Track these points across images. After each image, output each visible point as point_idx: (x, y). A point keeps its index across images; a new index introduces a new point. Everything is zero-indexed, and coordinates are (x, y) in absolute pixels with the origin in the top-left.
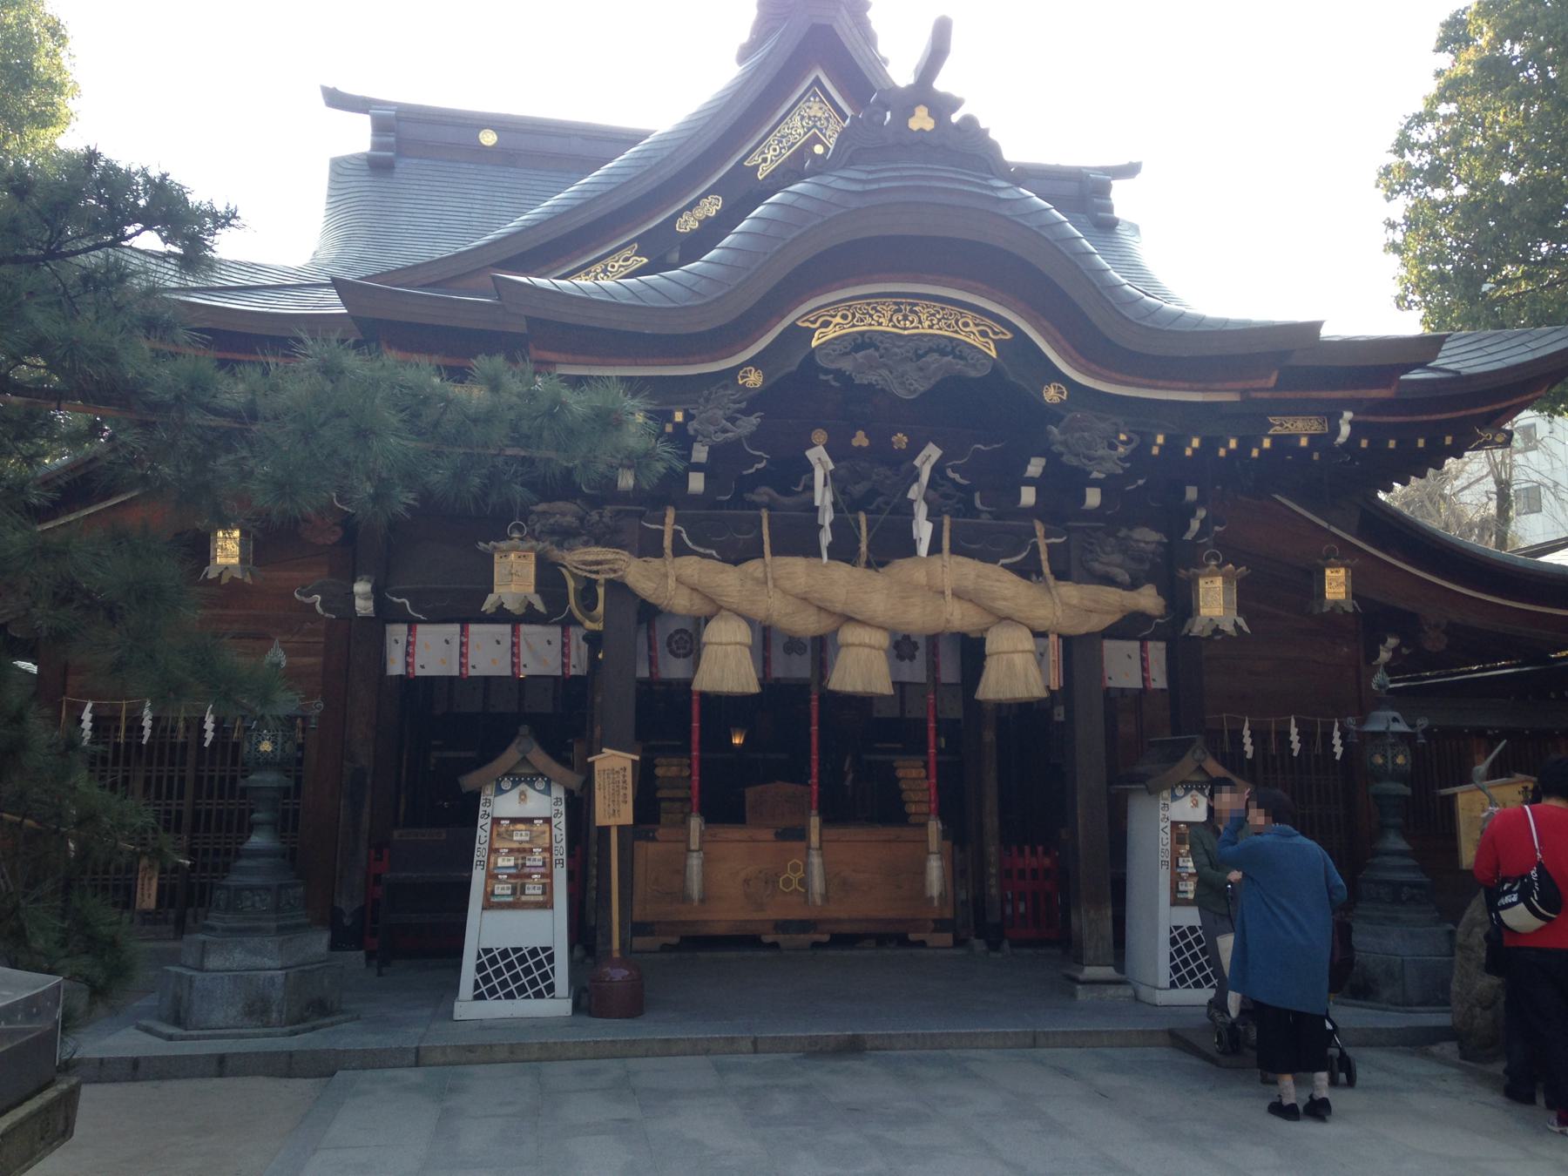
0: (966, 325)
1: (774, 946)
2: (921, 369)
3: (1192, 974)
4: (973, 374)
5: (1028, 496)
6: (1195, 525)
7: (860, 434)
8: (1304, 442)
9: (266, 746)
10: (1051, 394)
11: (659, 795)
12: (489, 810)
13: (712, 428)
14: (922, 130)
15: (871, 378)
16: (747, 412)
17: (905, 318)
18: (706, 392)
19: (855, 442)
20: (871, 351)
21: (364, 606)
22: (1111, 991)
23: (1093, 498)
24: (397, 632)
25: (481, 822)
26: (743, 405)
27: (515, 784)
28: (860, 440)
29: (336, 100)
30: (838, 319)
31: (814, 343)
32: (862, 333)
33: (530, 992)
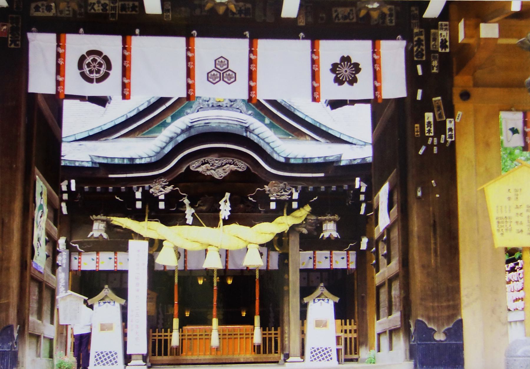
2: (224, 170)
4: (240, 170)
13: (157, 191)
15: (208, 173)
16: (169, 185)
20: (207, 165)
26: (167, 183)
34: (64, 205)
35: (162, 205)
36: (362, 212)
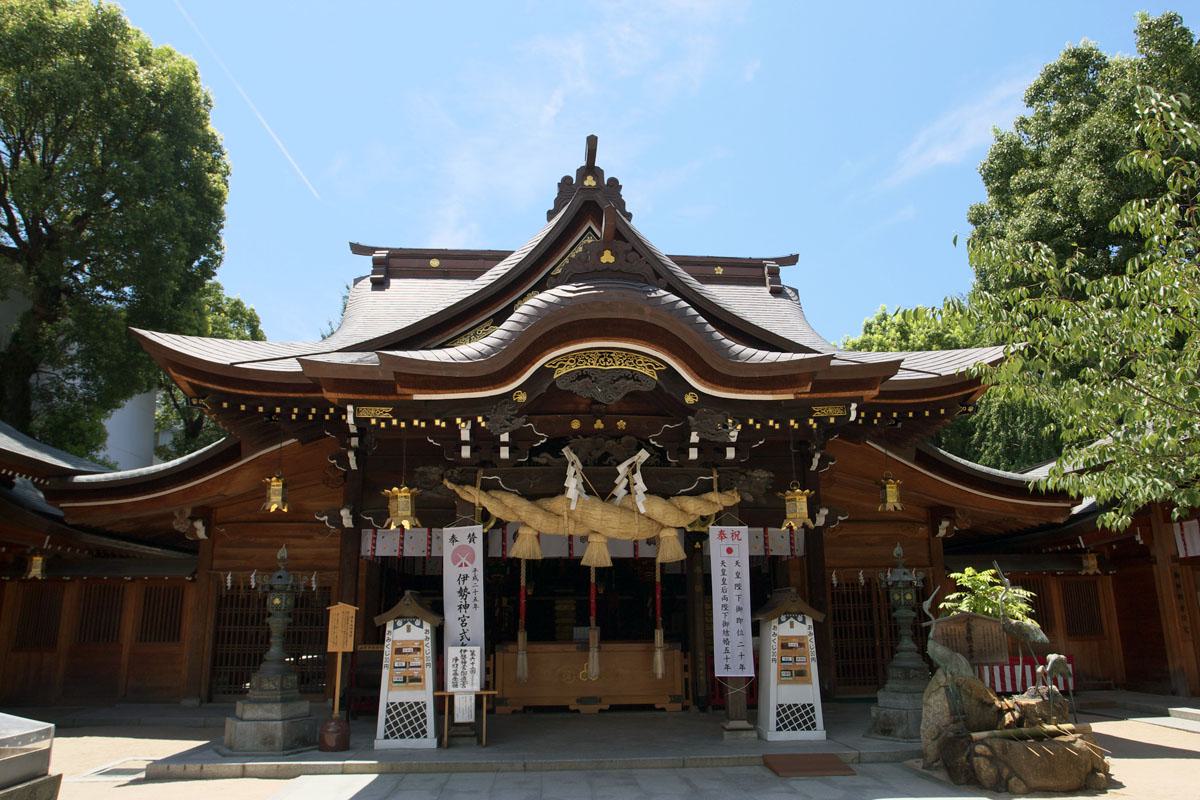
0: (640, 362)
1: (578, 711)
3: (791, 723)
4: (646, 389)
5: (693, 454)
6: (815, 462)
7: (599, 421)
8: (832, 420)
9: (277, 601)
10: (689, 399)
11: (557, 621)
12: (390, 637)
14: (607, 263)
16: (518, 416)
17: (606, 360)
18: (495, 407)
19: (596, 426)
20: (588, 379)
21: (348, 522)
22: (744, 734)
23: (731, 453)
24: (367, 534)
25: (386, 643)
26: (516, 412)
27: (404, 623)
28: (599, 425)
29: (357, 249)
30: (568, 363)
31: (555, 376)
32: (582, 370)
33: (397, 735)
34: (351, 455)
35: (505, 453)
36: (813, 468)
